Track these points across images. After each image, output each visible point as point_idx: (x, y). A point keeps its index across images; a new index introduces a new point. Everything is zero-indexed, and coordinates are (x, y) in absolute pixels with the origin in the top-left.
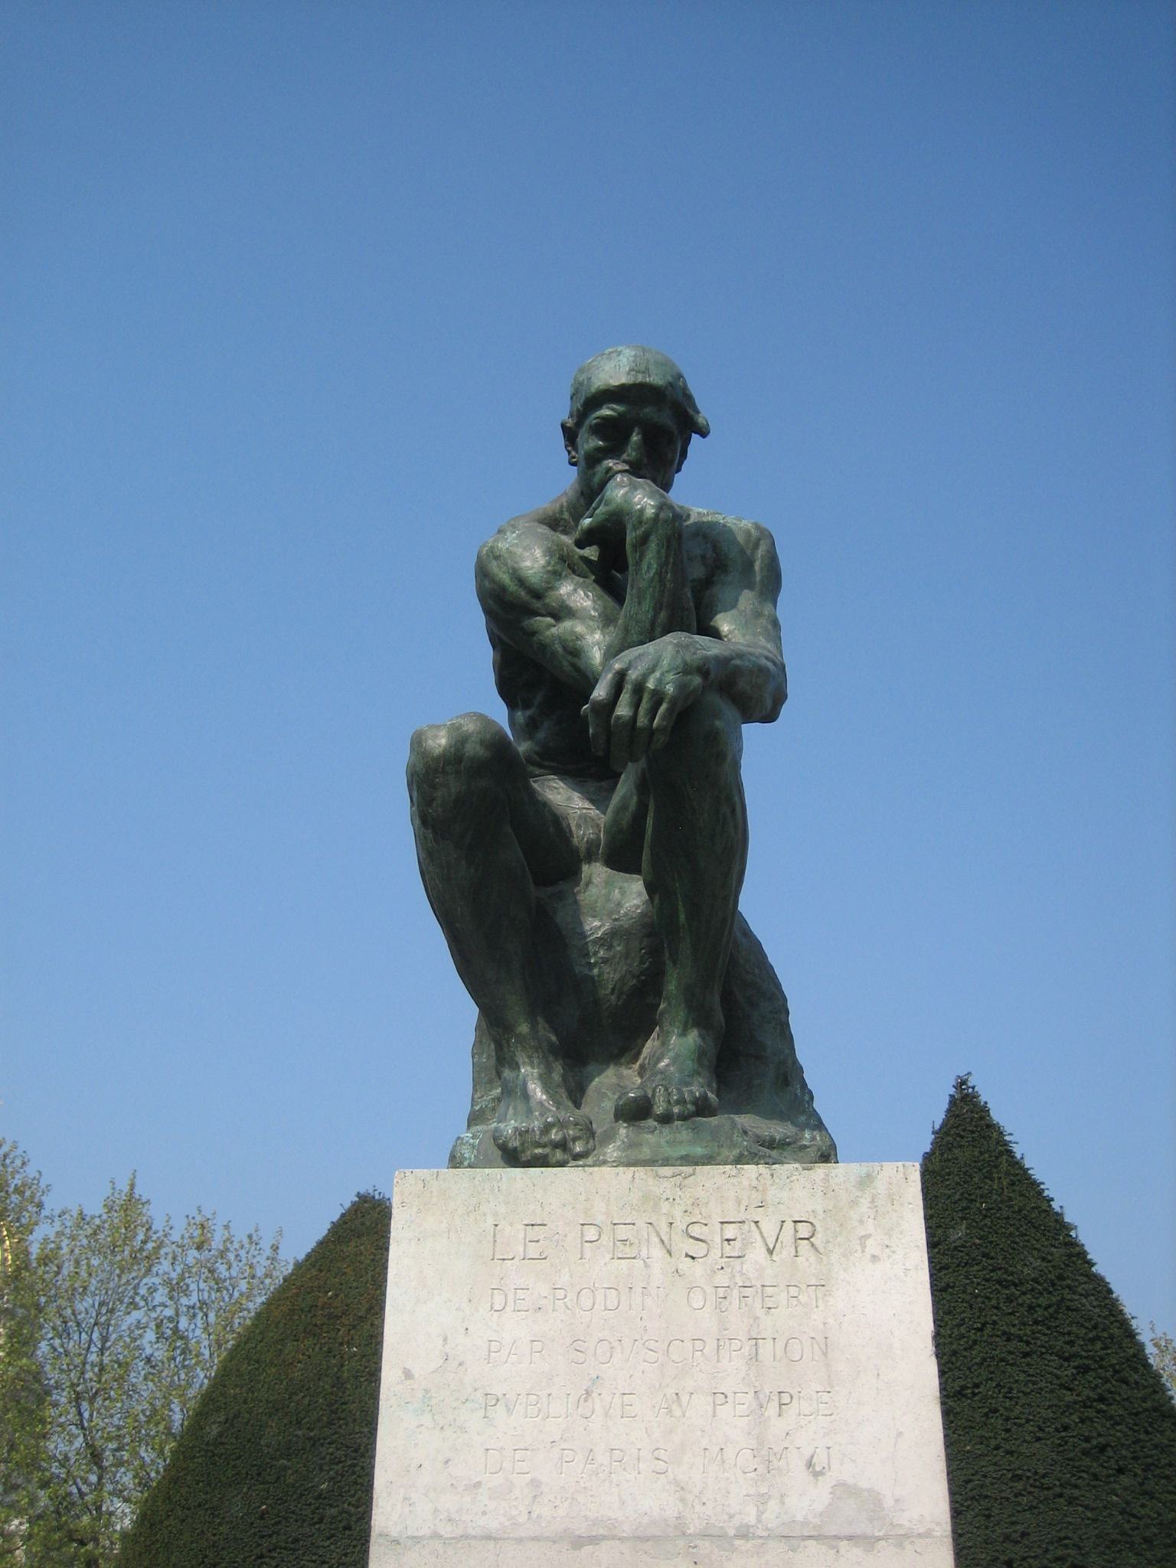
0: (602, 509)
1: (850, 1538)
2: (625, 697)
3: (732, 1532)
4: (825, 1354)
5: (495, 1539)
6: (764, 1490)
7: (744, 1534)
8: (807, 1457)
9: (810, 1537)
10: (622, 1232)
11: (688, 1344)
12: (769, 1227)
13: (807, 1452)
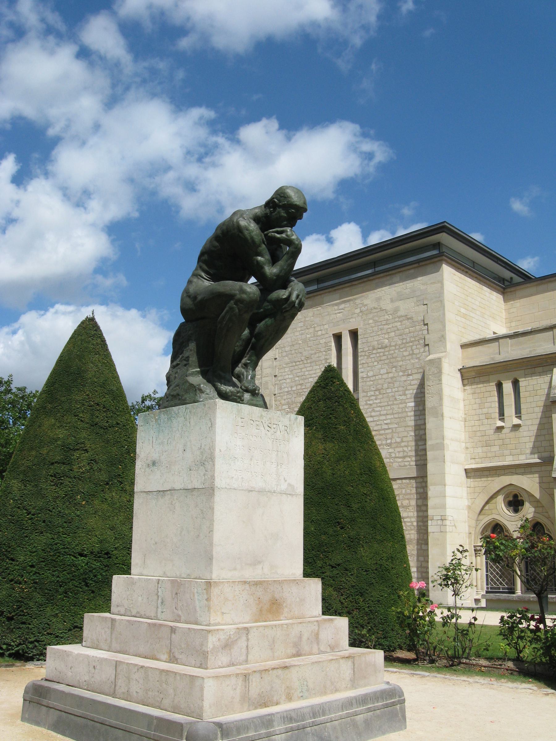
0: (284, 235)
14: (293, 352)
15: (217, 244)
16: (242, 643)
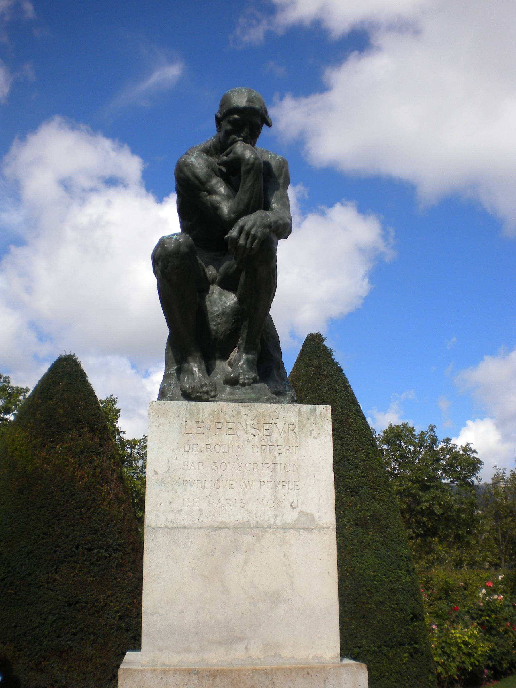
0: (231, 155)
1: (303, 529)
2: (243, 236)
3: (266, 526)
4: (298, 469)
5: (187, 528)
6: (276, 513)
7: (270, 527)
8: (291, 503)
9: (291, 528)
10: (230, 425)
11: (252, 465)
12: (280, 425)
13: (291, 501)
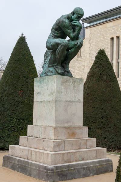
7: (74, 101)
12: (76, 82)
14: (96, 45)
15: (57, 26)
16: (63, 145)
